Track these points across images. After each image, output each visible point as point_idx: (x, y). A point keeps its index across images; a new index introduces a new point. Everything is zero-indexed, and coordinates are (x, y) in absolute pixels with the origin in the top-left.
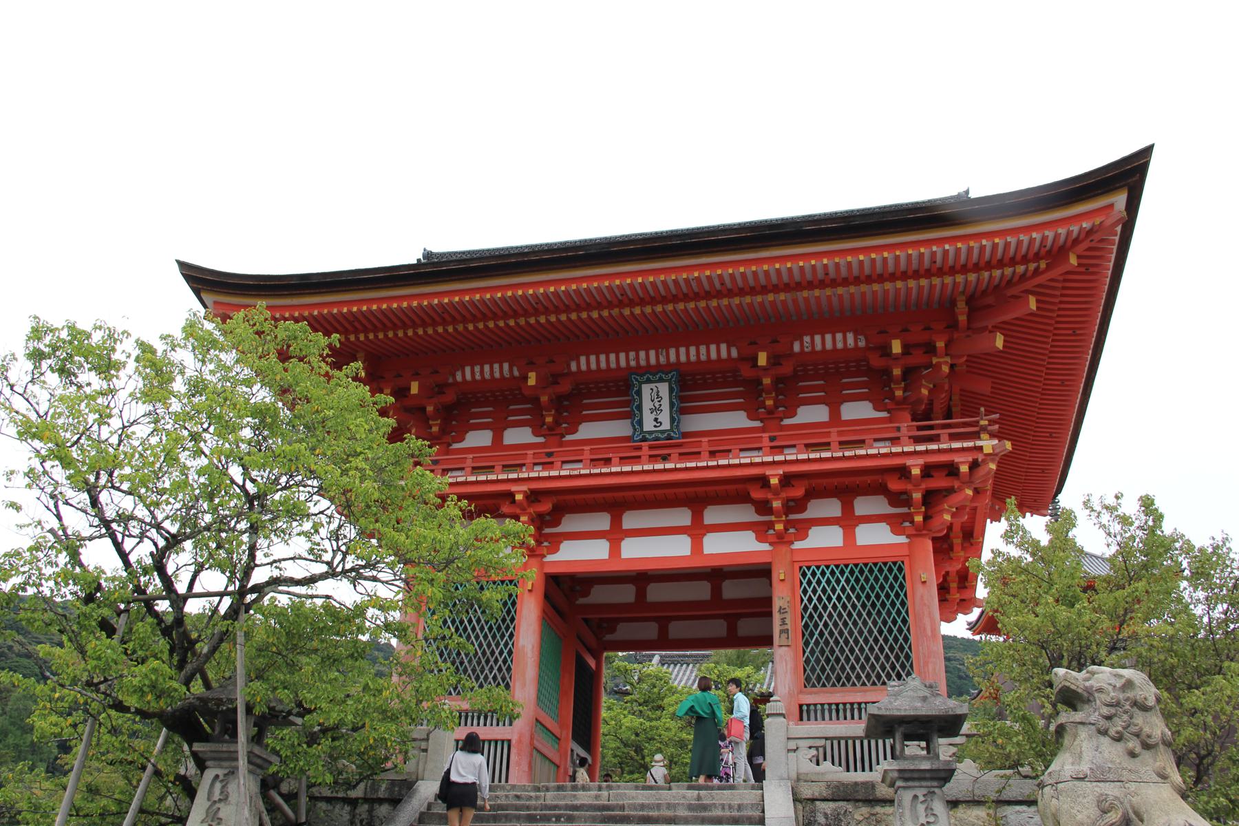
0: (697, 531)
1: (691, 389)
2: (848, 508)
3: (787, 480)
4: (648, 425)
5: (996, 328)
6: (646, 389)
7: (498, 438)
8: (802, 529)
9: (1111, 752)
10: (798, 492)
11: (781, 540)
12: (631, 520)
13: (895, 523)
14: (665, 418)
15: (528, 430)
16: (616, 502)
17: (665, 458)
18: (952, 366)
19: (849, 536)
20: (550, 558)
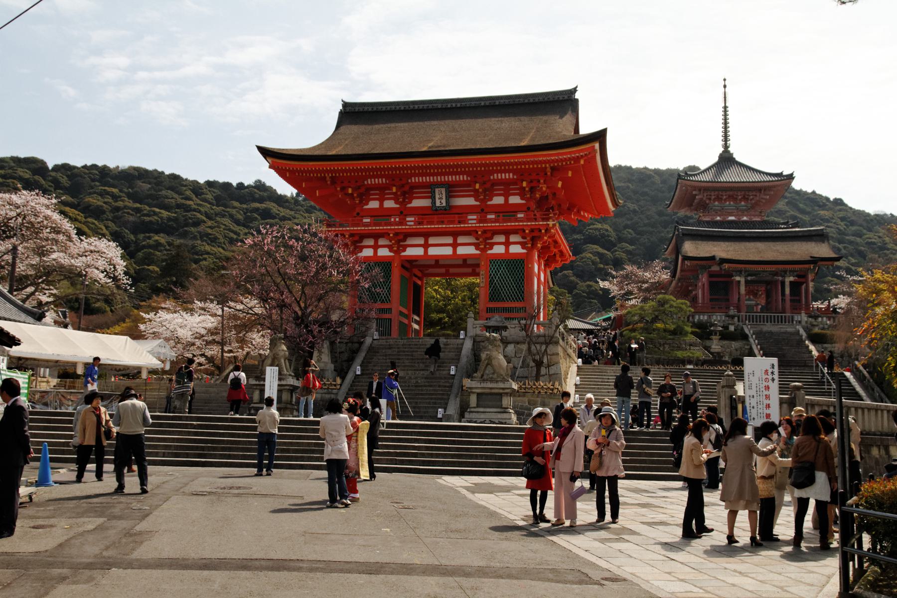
0: (455, 245)
1: (452, 190)
2: (507, 239)
3: (485, 232)
4: (438, 204)
5: (559, 180)
6: (437, 190)
7: (381, 204)
8: (491, 246)
9: (490, 347)
10: (489, 235)
11: (484, 250)
12: (432, 241)
13: (523, 245)
14: (444, 201)
15: (393, 202)
16: (426, 235)
17: (442, 223)
18: (548, 187)
19: (507, 249)
20: (403, 254)
